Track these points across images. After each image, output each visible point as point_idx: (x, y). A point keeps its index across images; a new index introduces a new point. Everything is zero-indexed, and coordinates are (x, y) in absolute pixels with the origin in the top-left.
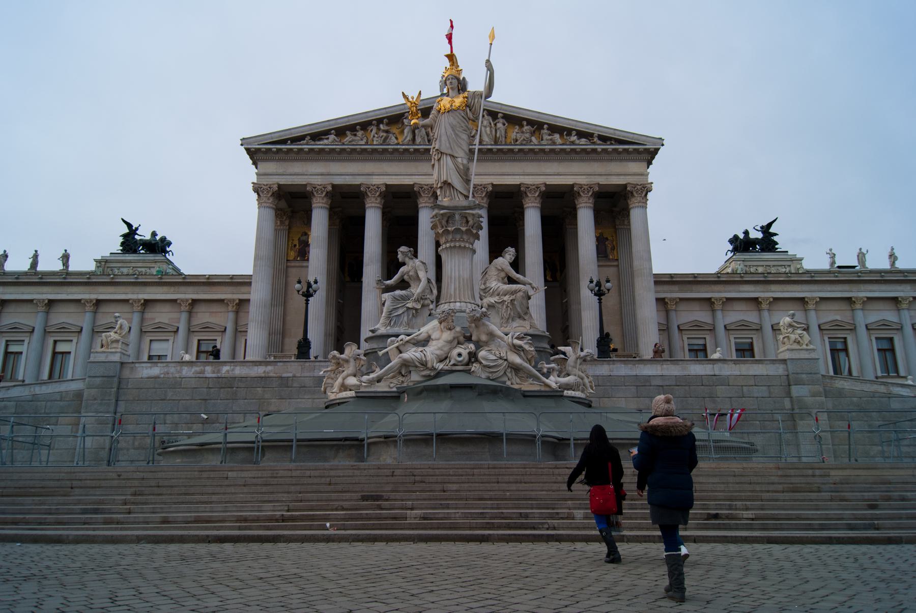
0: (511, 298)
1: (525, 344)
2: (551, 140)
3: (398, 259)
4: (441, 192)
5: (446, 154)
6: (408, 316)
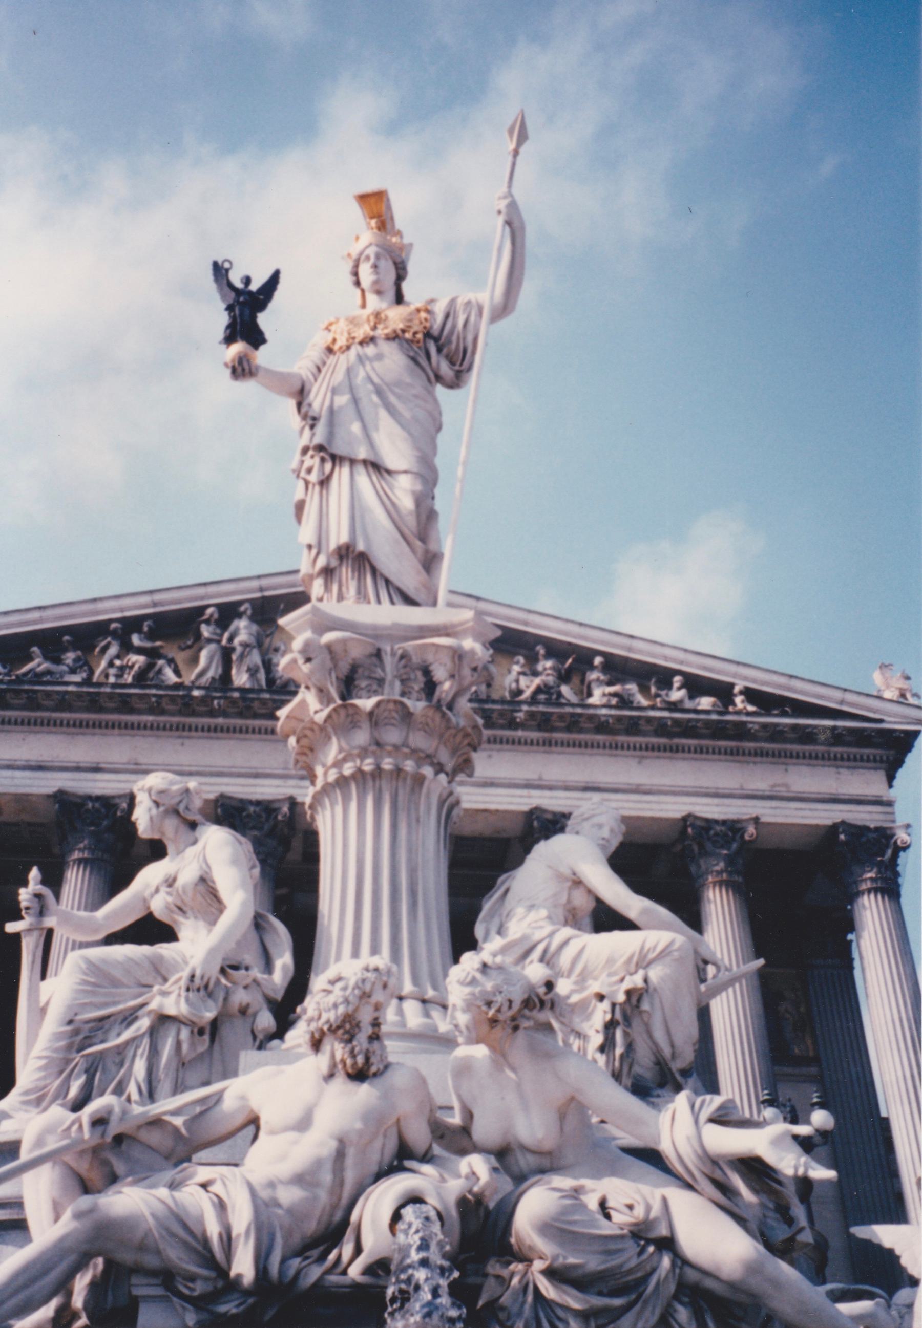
0: (627, 985)
1: (776, 1142)
2: (615, 695)
3: (133, 826)
4: (327, 588)
5: (353, 462)
6: (154, 1053)
